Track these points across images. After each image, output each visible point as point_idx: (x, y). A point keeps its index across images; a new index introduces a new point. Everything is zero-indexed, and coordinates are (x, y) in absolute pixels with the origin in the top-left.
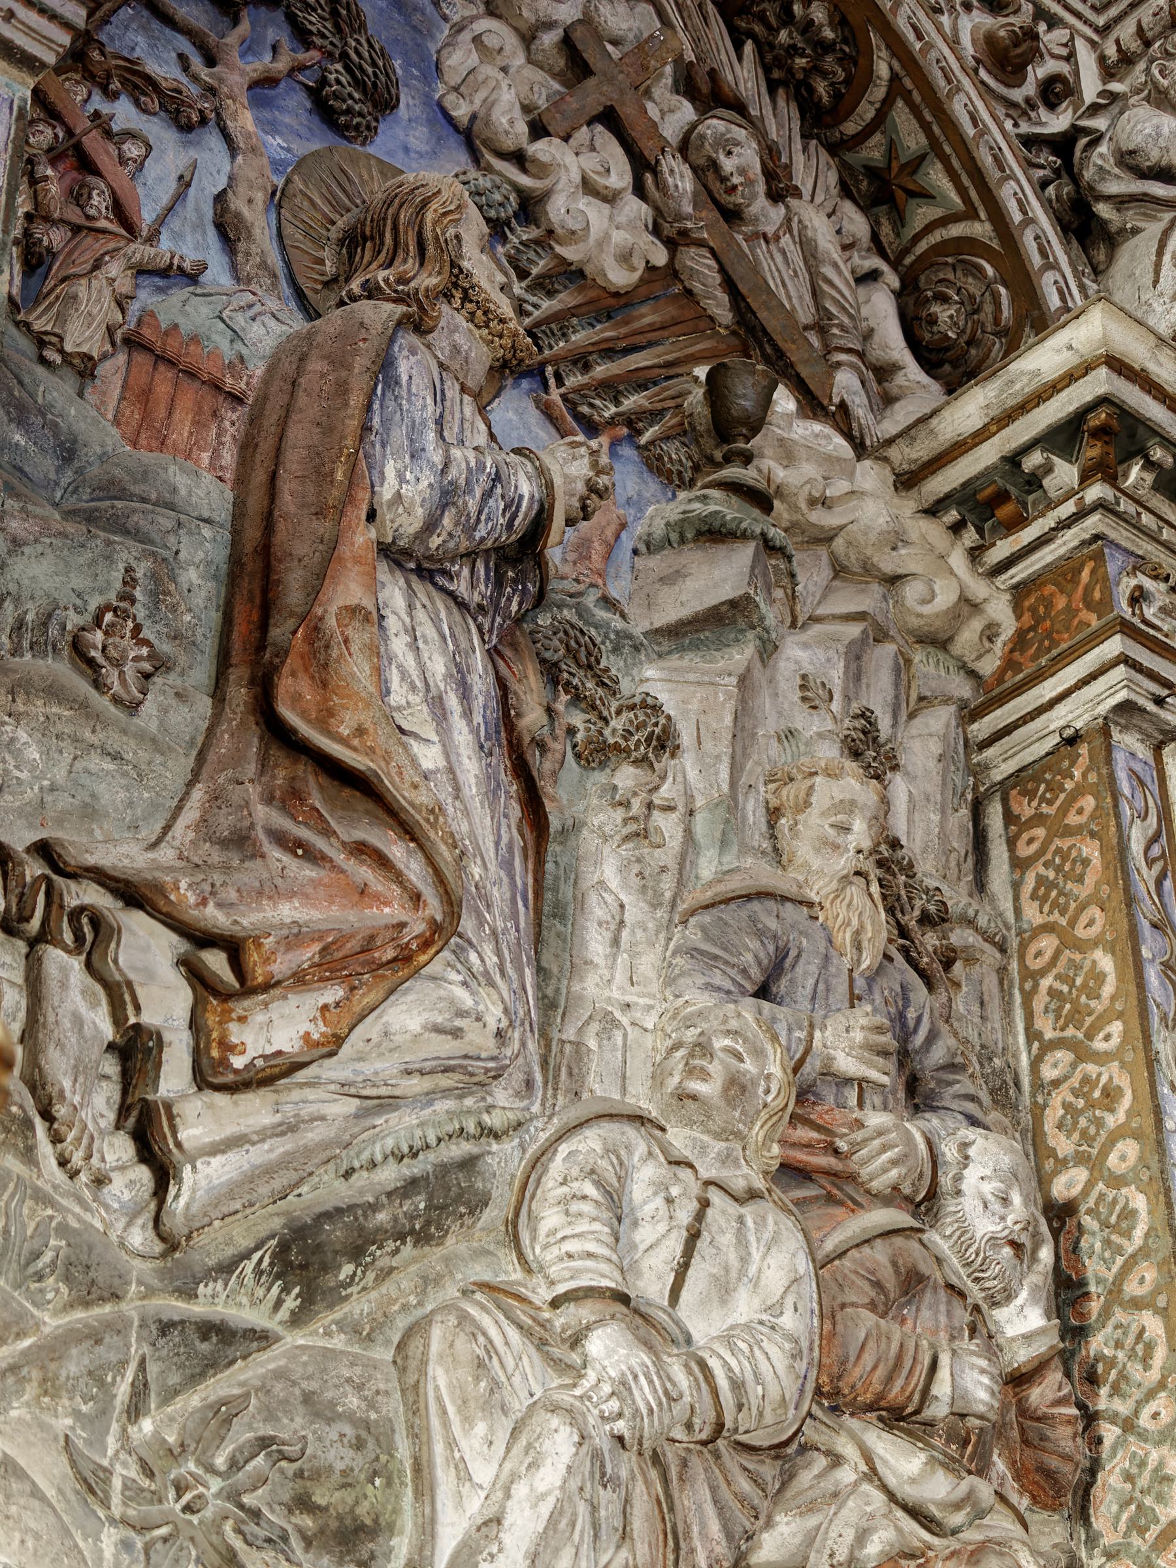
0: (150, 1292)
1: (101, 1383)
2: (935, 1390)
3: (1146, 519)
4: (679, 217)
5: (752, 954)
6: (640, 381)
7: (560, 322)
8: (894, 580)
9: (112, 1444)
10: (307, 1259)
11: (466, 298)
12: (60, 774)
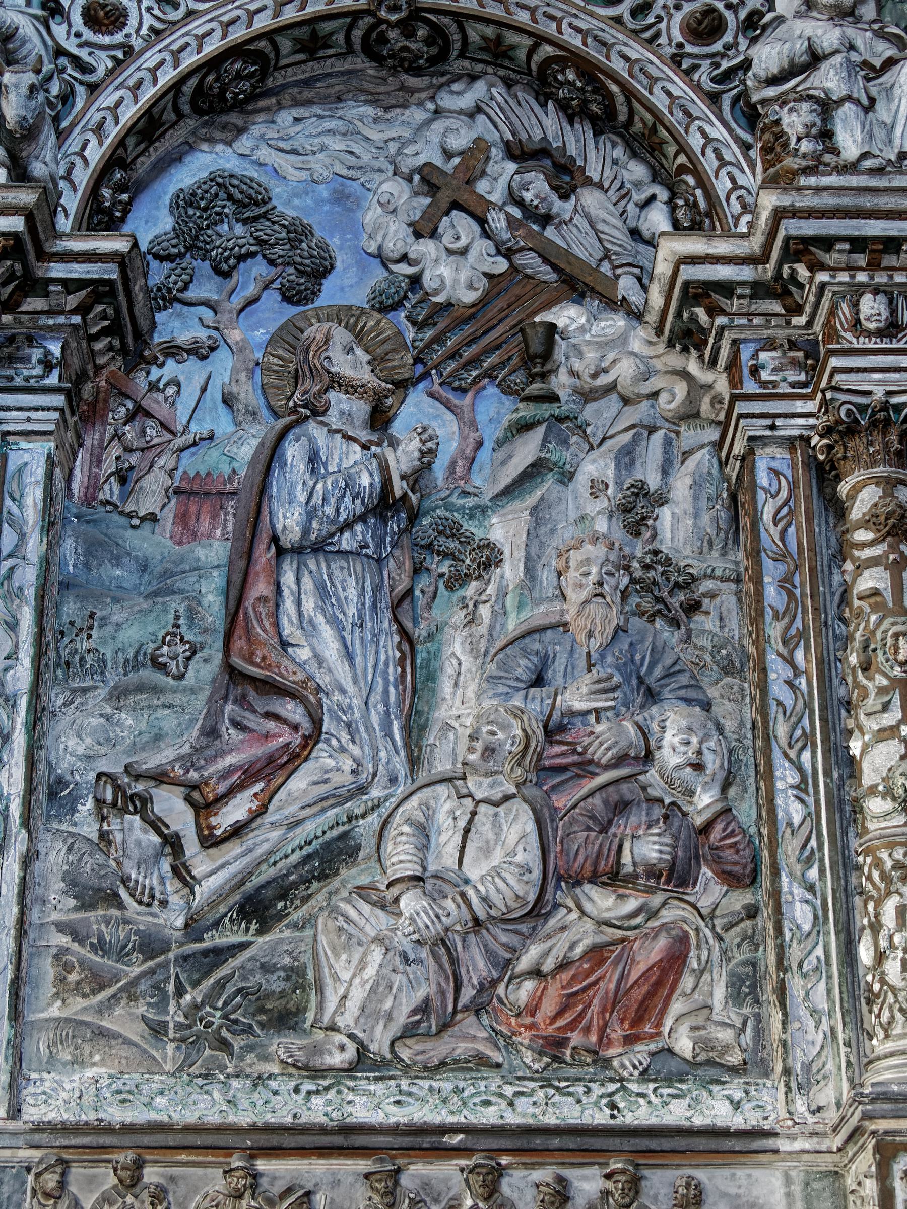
0: (182, 944)
1: (159, 989)
2: (623, 861)
3: (756, 321)
4: (504, 243)
5: (523, 668)
6: (488, 350)
7: (439, 339)
8: (655, 395)
9: (172, 1009)
10: (259, 906)
11: (340, 386)
12: (143, 726)
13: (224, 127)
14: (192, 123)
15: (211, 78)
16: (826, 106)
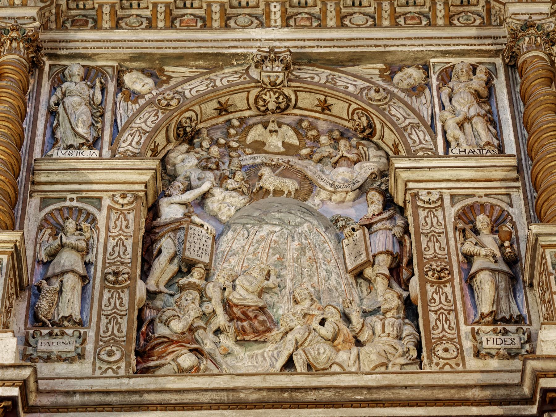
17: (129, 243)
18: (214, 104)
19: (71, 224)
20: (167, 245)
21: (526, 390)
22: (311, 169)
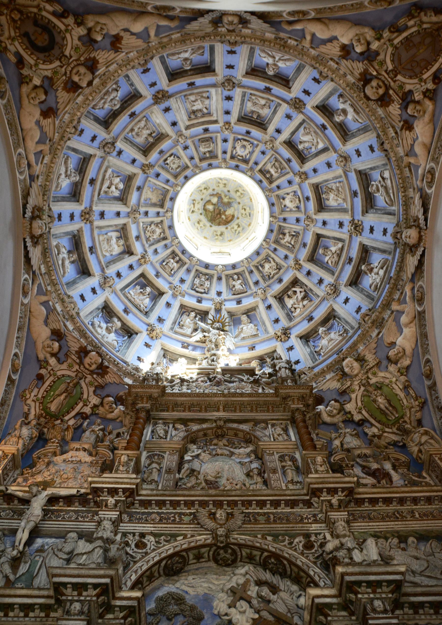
13: (173, 580)
14: (162, 578)
15: (169, 562)
16: (349, 550)
17: (174, 463)
18: (202, 433)
19: (156, 457)
20: (186, 466)
21: (305, 491)
22: (232, 450)
